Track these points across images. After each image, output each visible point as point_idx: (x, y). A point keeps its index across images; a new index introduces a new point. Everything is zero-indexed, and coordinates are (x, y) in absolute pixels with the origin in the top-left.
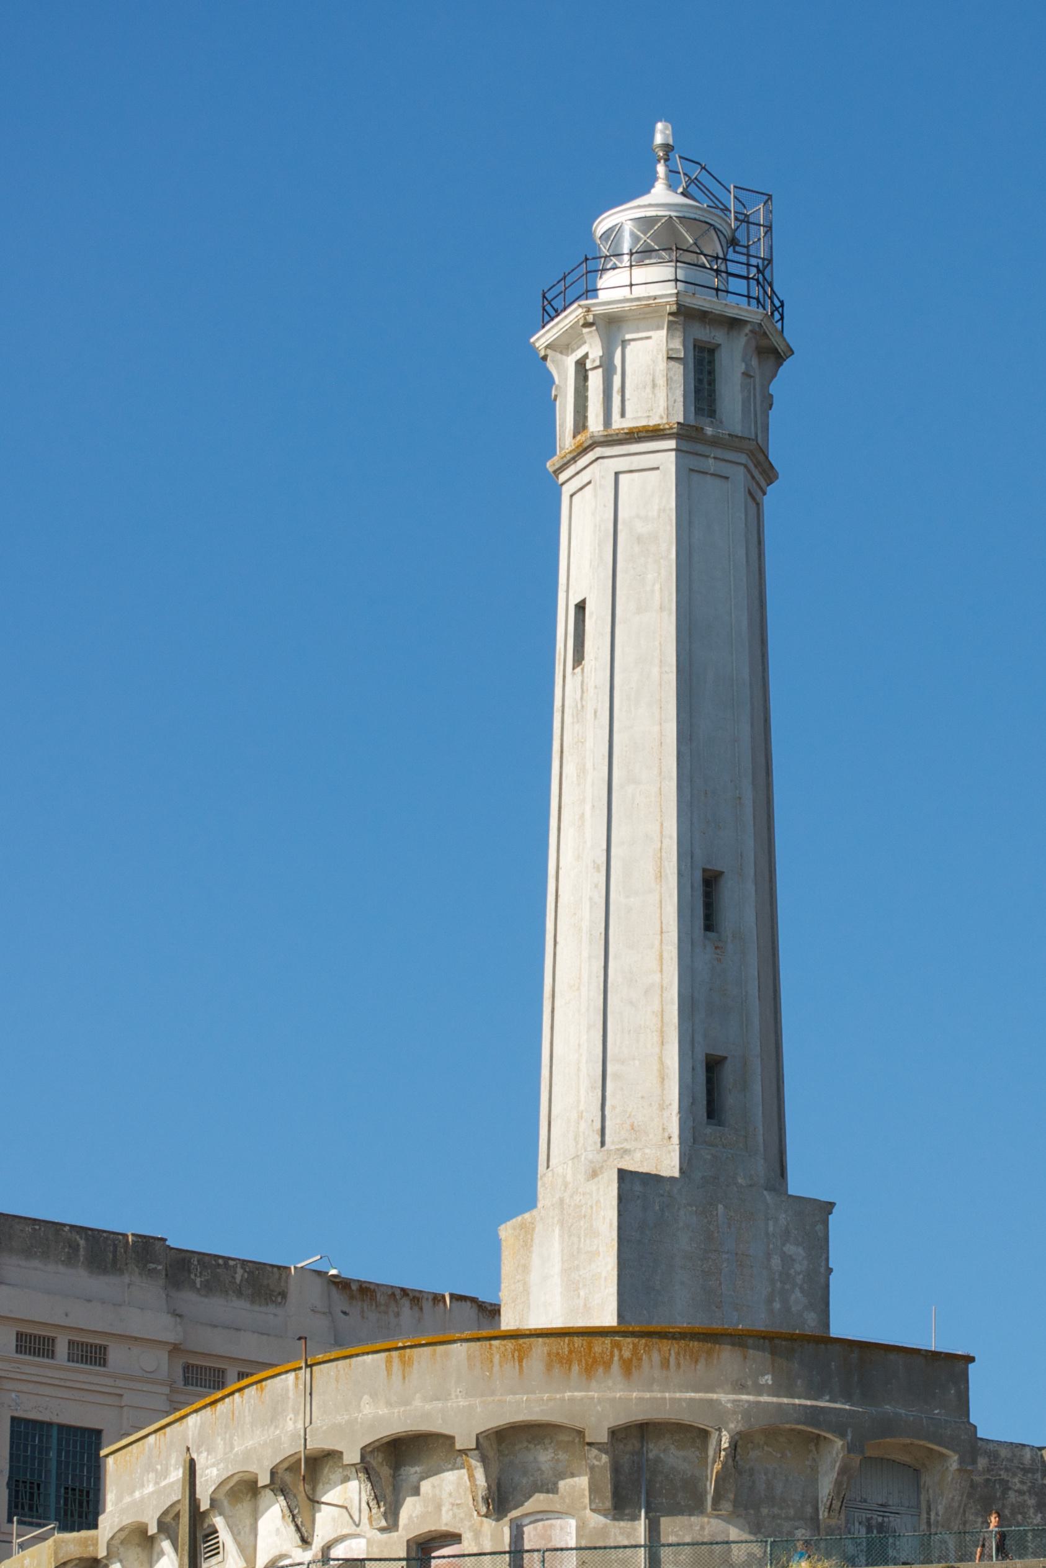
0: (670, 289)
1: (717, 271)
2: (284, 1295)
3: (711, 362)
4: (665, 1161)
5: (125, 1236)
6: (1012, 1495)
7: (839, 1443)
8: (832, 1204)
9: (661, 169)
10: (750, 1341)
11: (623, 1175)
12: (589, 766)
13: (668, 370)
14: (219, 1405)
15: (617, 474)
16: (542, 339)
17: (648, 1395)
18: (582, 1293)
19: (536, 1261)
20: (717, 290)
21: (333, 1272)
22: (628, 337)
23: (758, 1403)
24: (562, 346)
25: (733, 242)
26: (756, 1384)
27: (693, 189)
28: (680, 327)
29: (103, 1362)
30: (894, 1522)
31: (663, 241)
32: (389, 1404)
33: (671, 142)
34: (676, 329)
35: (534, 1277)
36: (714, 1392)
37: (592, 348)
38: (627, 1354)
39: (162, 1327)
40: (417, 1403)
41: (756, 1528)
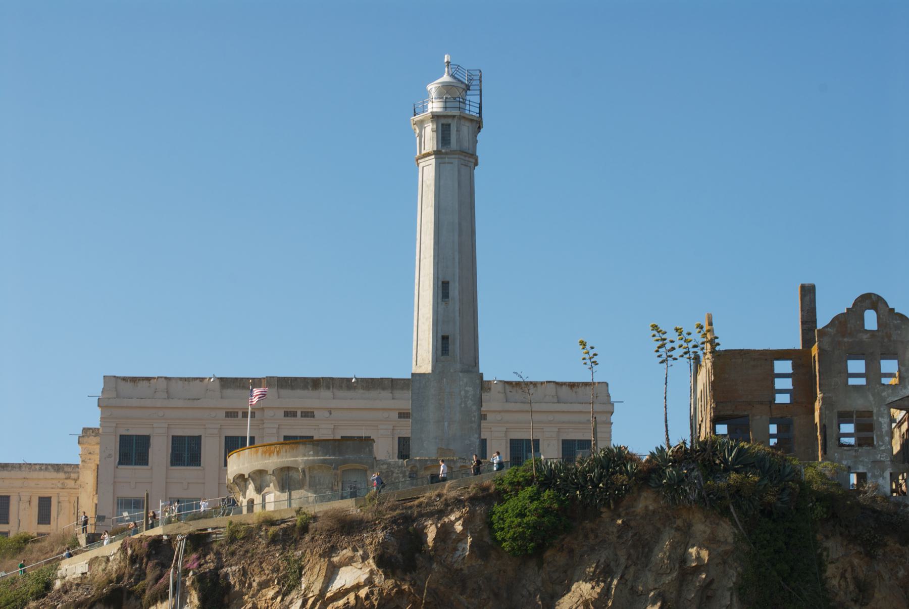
2: (490, 389)
6: (395, 475)
30: (359, 486)
41: (315, 492)
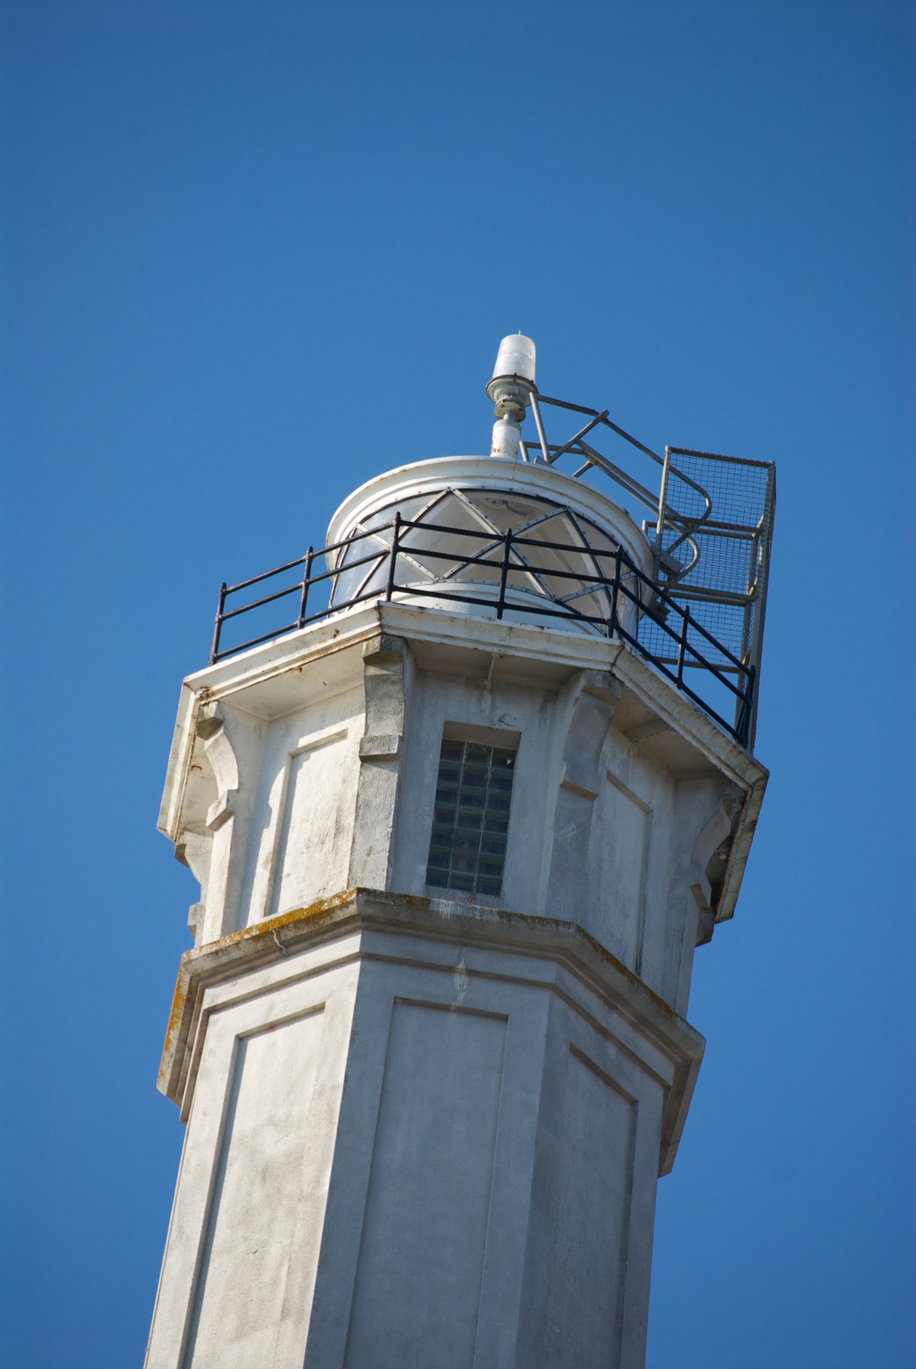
13: (363, 785)
22: (303, 742)
28: (395, 689)
33: (531, 375)
34: (388, 696)
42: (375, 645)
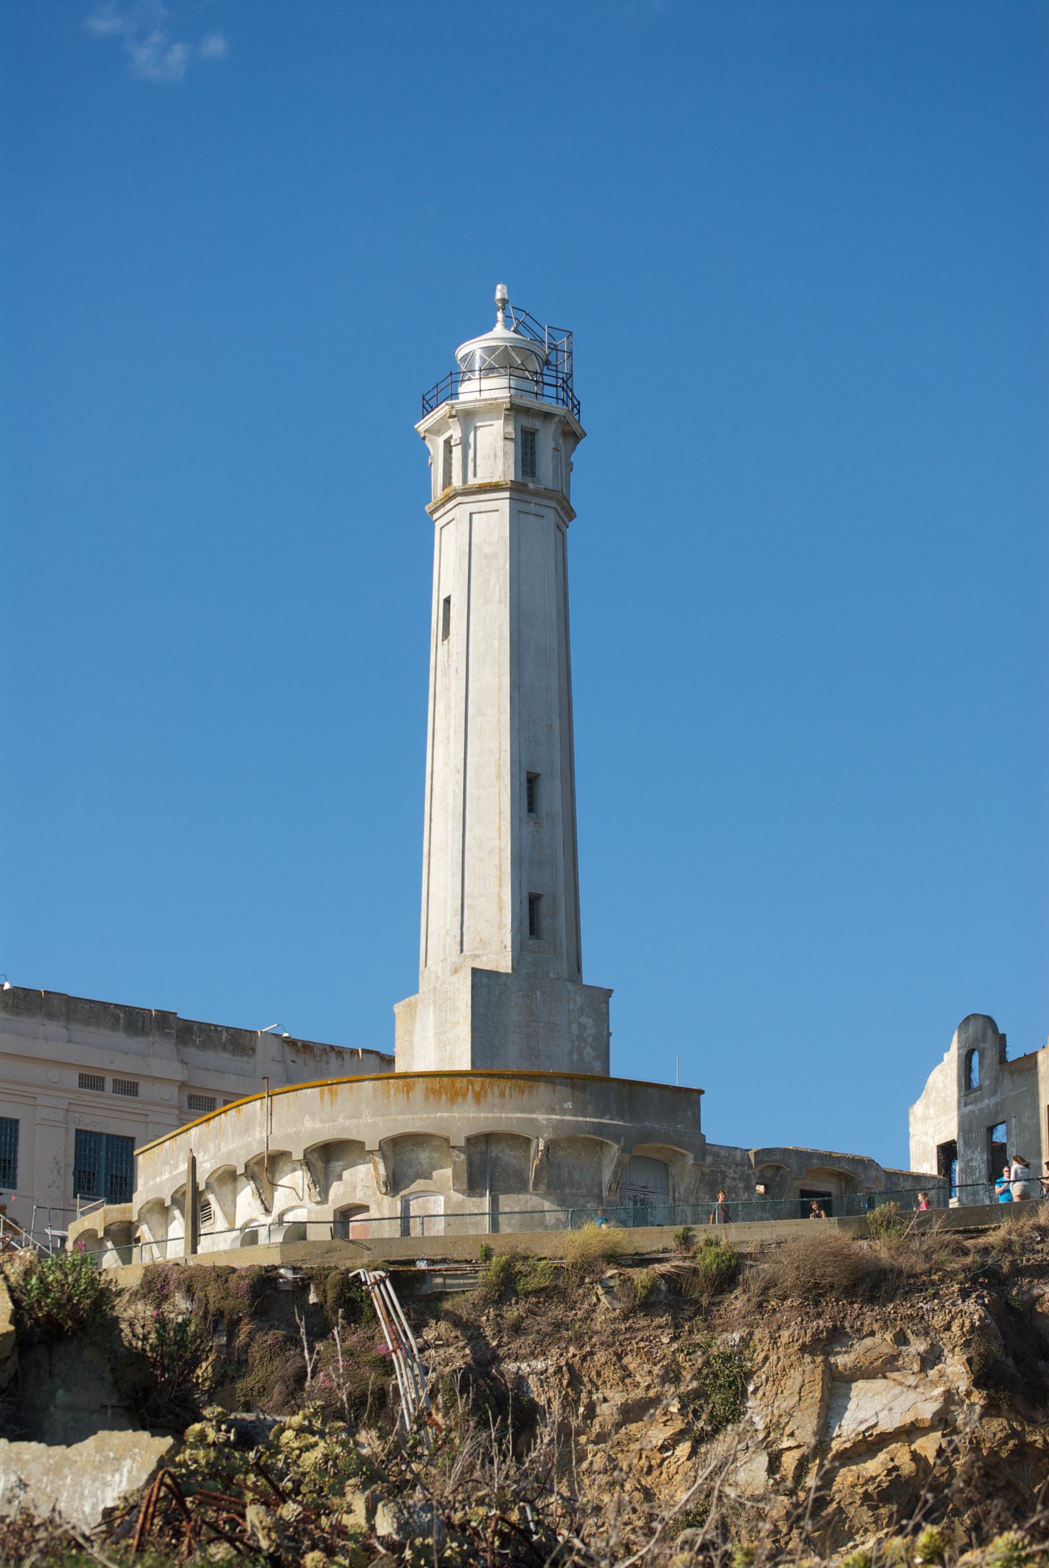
0: (506, 393)
1: (537, 382)
2: (253, 1050)
3: (533, 441)
4: (504, 963)
5: (150, 1011)
6: (728, 1180)
7: (616, 1147)
8: (611, 991)
9: (500, 315)
10: (558, 1080)
11: (475, 972)
12: (453, 704)
14: (212, 1122)
15: (471, 514)
16: (422, 426)
17: (491, 1115)
18: (448, 1048)
19: (418, 1027)
20: (537, 394)
21: (286, 1035)
22: (478, 424)
23: (563, 1120)
24: (435, 430)
25: (547, 363)
26: (561, 1108)
27: (521, 328)
29: (135, 1093)
30: (652, 1198)
31: (502, 362)
32: (322, 1121)
35: (417, 1038)
36: (533, 1113)
37: (455, 432)
38: (477, 1088)
39: (173, 1070)
40: (341, 1120)
41: (562, 1202)
42: (508, 406)
